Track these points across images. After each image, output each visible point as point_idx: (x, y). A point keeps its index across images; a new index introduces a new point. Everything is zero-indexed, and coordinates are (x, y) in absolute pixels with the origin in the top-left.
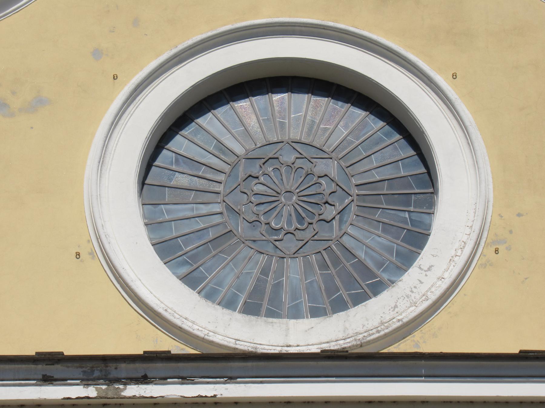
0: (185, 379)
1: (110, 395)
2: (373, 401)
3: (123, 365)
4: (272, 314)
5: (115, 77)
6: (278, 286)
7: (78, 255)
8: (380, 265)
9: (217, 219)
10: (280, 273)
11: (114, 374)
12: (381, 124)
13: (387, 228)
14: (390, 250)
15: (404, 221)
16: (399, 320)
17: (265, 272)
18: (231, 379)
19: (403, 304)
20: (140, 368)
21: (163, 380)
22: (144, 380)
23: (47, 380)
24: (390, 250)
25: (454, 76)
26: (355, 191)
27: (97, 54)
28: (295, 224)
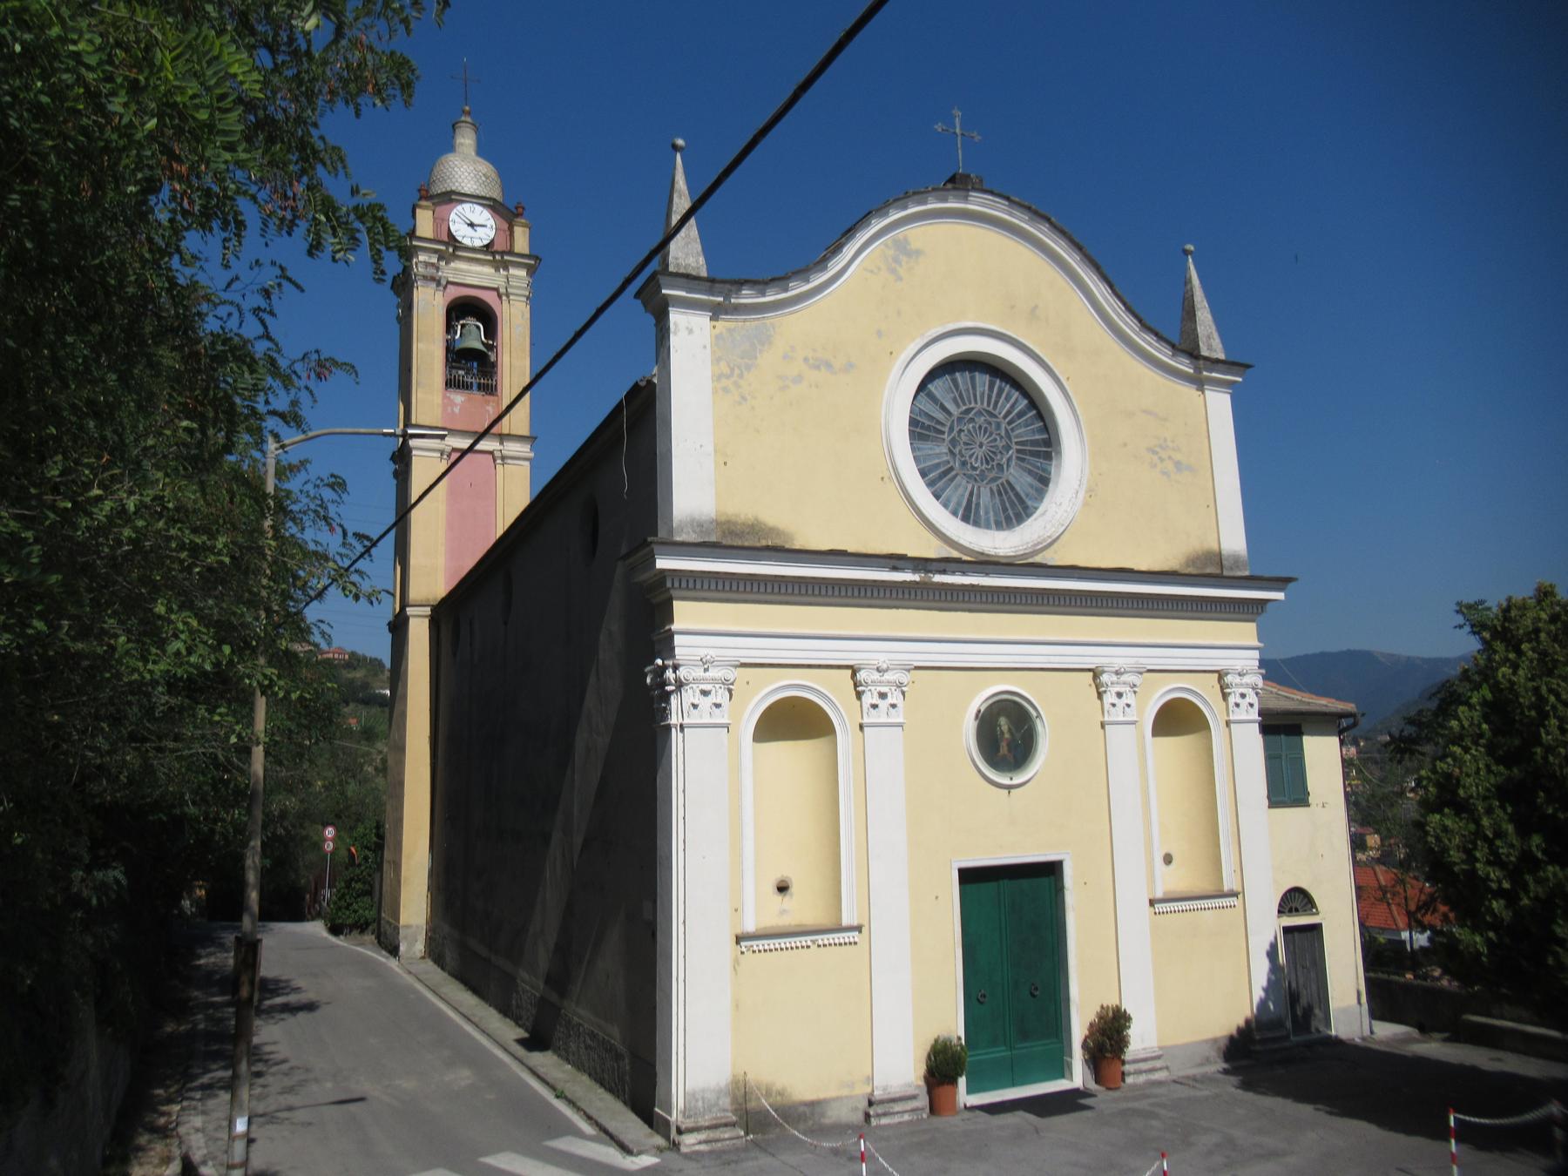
0: (964, 573)
1: (926, 580)
2: (445, 344)
3: (934, 564)
4: (976, 524)
5: (891, 353)
6: (978, 505)
7: (882, 478)
8: (1027, 495)
9: (945, 458)
10: (979, 496)
11: (929, 568)
12: (1026, 402)
13: (1030, 472)
14: (1032, 486)
15: (1038, 468)
16: (1049, 537)
17: (971, 494)
18: (987, 574)
19: (1048, 526)
20: (942, 566)
21: (953, 573)
22: (944, 572)
23: (895, 569)
24: (1032, 486)
25: (1068, 379)
26: (1015, 447)
27: (879, 333)
28: (985, 466)
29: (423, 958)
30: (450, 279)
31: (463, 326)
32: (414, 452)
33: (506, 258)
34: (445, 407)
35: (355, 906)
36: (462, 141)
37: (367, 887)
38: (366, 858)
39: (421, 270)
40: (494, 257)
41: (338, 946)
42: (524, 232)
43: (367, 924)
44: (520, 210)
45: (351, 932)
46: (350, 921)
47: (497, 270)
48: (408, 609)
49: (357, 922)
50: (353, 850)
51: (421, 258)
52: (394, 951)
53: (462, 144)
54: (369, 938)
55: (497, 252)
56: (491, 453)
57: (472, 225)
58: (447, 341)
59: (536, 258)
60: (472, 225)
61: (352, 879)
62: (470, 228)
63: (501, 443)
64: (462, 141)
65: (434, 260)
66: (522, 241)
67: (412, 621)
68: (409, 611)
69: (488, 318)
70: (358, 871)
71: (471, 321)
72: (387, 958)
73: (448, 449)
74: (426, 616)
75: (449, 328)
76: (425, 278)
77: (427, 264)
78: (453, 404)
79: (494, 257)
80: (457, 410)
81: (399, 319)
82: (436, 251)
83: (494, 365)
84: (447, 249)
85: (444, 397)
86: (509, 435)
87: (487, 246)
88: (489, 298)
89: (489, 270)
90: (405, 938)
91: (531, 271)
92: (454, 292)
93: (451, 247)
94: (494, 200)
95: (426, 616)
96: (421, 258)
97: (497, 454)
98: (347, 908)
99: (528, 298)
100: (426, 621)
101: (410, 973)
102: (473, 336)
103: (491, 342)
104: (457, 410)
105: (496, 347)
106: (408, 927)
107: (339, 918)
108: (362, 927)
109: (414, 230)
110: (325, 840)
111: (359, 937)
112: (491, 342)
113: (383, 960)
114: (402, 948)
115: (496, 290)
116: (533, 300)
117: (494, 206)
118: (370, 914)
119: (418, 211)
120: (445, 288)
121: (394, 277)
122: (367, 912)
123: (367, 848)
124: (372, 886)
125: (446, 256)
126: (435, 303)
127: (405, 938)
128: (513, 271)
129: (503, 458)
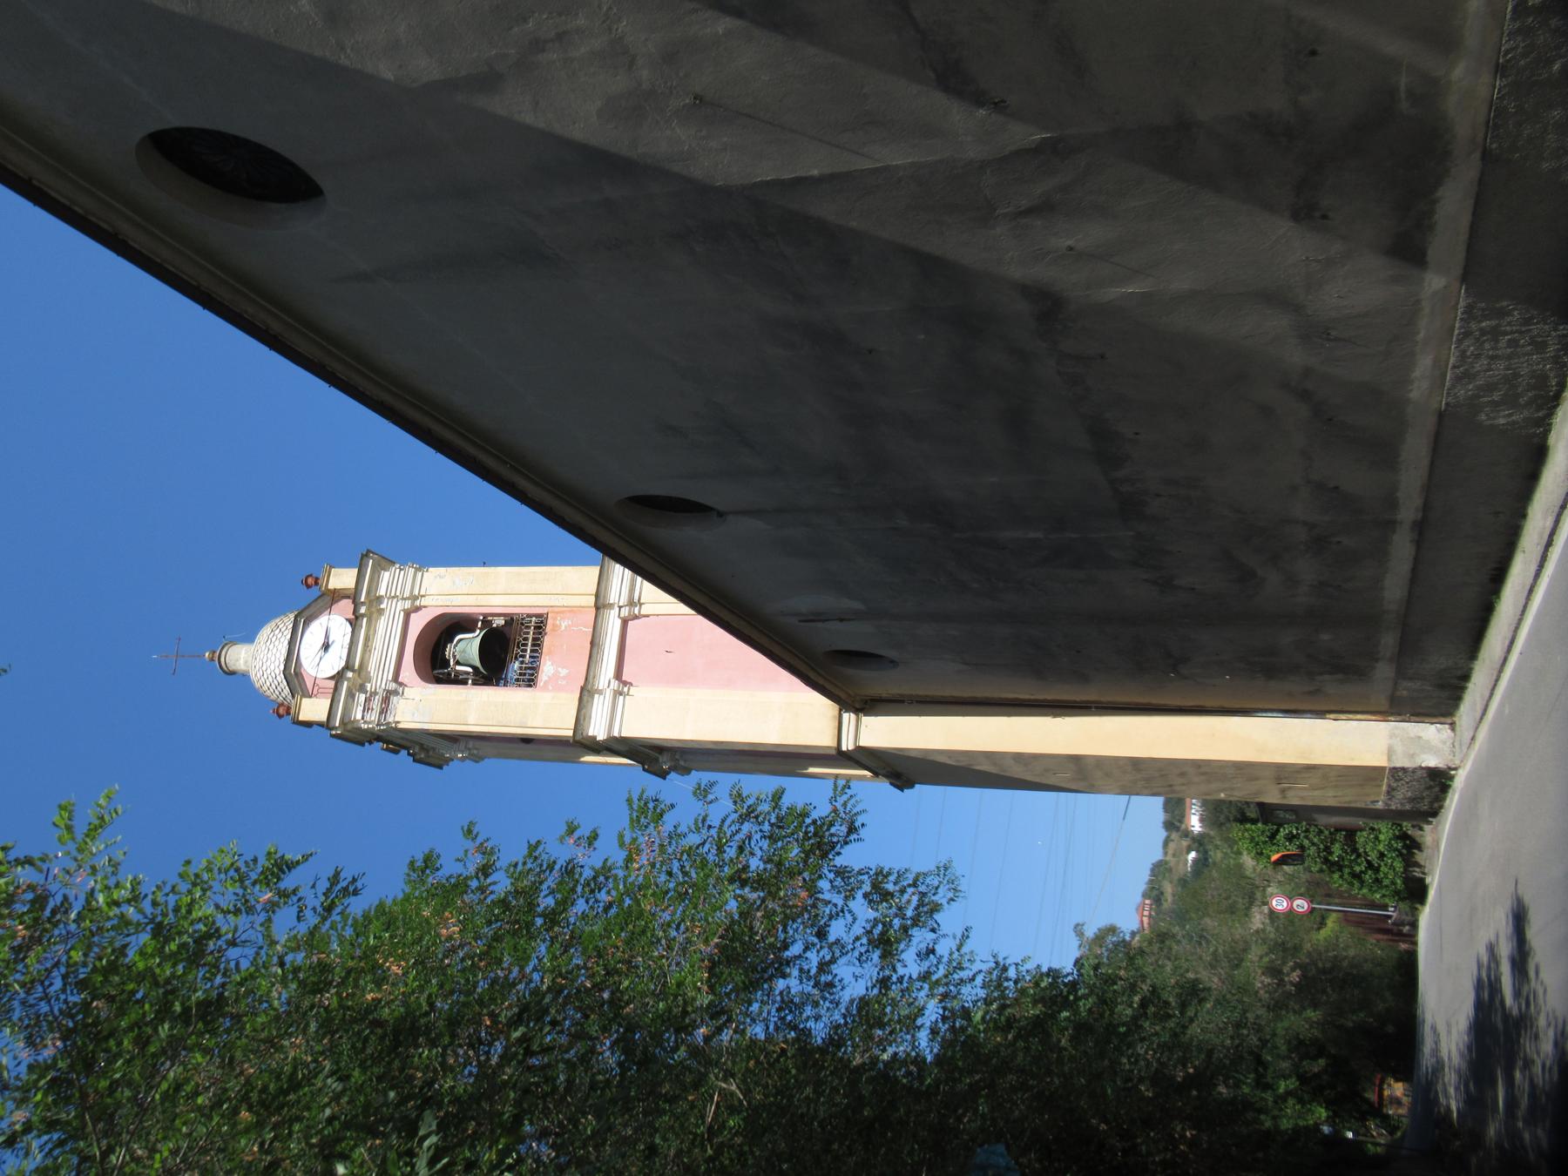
29: (1453, 725)
30: (390, 678)
31: (458, 663)
32: (616, 734)
33: (362, 600)
34: (559, 689)
35: (1373, 856)
36: (242, 662)
37: (1341, 836)
38: (1290, 838)
39: (373, 716)
40: (363, 616)
41: (1440, 882)
42: (335, 575)
43: (1404, 837)
44: (310, 581)
45: (1419, 866)
46: (1399, 865)
47: (381, 612)
48: (844, 748)
49: (1401, 854)
50: (1275, 857)
51: (358, 714)
52: (1439, 780)
53: (246, 662)
54: (1427, 835)
55: (355, 612)
56: (625, 622)
57: (326, 647)
58: (474, 684)
59: (365, 556)
60: (326, 647)
61: (1326, 861)
62: (331, 650)
63: (611, 606)
64: (242, 662)
65: (363, 697)
66: (343, 578)
67: (863, 743)
68: (848, 745)
69: (449, 627)
70: (1312, 851)
71: (450, 651)
72: (1454, 791)
73: (615, 684)
74: (858, 721)
75: (458, 680)
76: (383, 711)
77: (366, 709)
78: (556, 676)
79: (363, 616)
80: (563, 672)
81: (477, 759)
82: (351, 695)
83: (511, 620)
84: (349, 679)
85: (545, 688)
86: (597, 596)
87: (351, 624)
88: (418, 623)
89: (382, 624)
90: (1412, 756)
91: (386, 562)
92: (409, 671)
93: (351, 675)
94: (296, 617)
95: (858, 721)
96: (359, 716)
97: (625, 612)
98: (1377, 870)
99: (417, 570)
100: (867, 720)
101: (1473, 738)
102: (467, 647)
103: (480, 624)
104: (563, 672)
105: (485, 616)
106: (1390, 753)
107: (1393, 883)
108: (1409, 847)
109: (320, 724)
110: (1291, 910)
111: (1427, 852)
112: (480, 624)
113: (1456, 797)
114: (1432, 762)
115: (407, 615)
116: (425, 561)
117: (305, 617)
118: (1386, 831)
119: (301, 718)
120: (401, 684)
121: (414, 761)
122: (1382, 837)
123: (1273, 836)
124: (1338, 830)
125: (360, 681)
126: (417, 699)
127: (1412, 756)
128: (382, 592)
129: (631, 603)
